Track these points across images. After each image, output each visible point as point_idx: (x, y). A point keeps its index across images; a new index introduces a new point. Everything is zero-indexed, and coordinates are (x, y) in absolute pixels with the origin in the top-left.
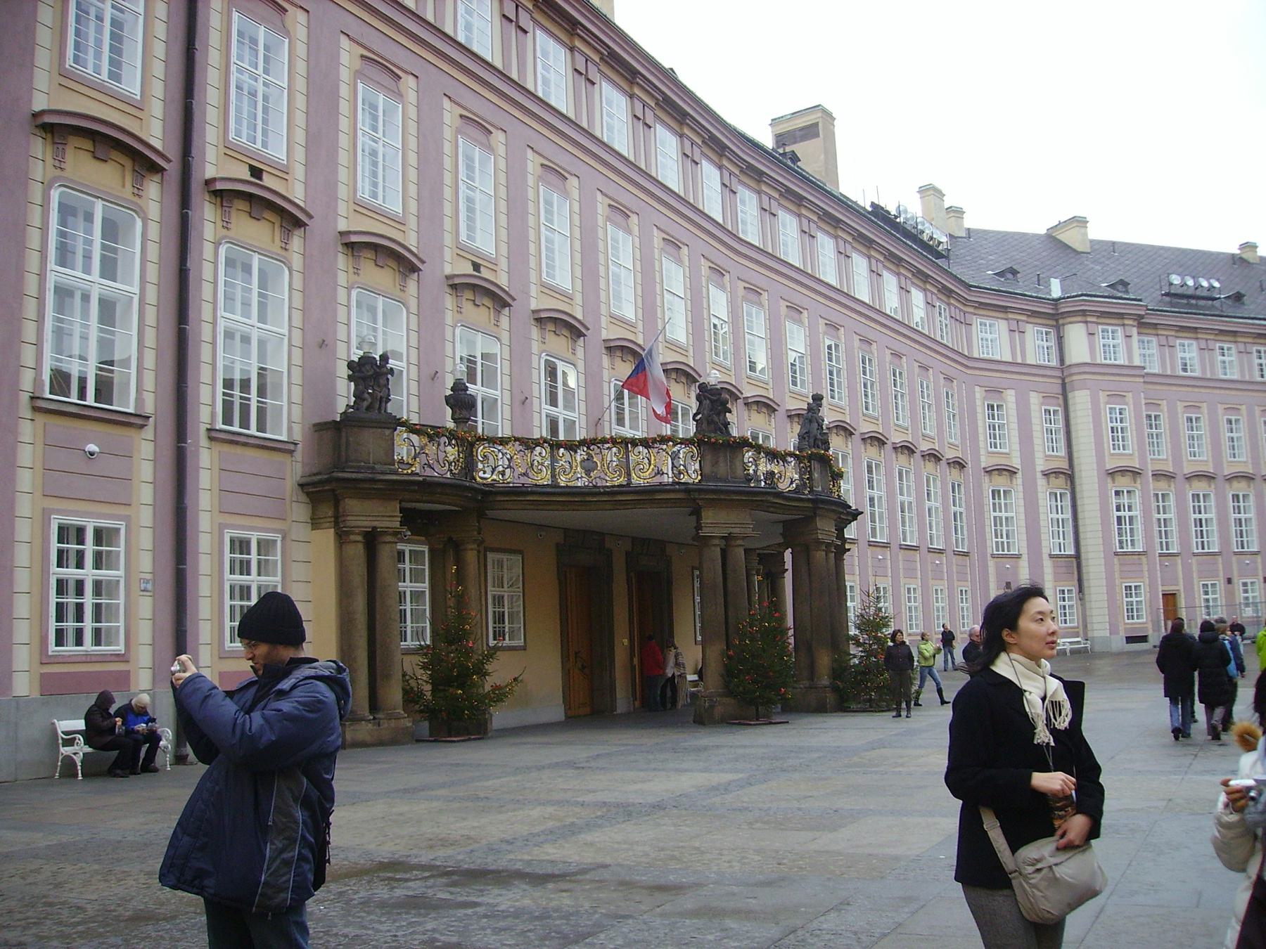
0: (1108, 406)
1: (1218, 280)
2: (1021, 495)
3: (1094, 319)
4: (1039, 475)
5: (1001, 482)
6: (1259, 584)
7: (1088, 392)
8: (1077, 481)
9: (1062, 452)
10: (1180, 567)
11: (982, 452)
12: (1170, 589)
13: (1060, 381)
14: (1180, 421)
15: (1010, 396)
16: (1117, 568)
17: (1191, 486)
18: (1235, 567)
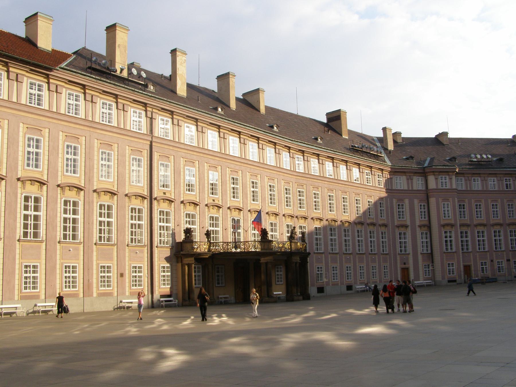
0: (442, 203)
1: (490, 155)
2: (410, 234)
3: (438, 174)
4: (417, 227)
5: (402, 230)
6: (505, 262)
7: (435, 199)
8: (432, 229)
9: (427, 219)
10: (472, 256)
11: (396, 220)
12: (467, 264)
13: (426, 195)
14: (473, 206)
15: (407, 201)
16: (445, 257)
17: (477, 228)
18: (494, 256)
